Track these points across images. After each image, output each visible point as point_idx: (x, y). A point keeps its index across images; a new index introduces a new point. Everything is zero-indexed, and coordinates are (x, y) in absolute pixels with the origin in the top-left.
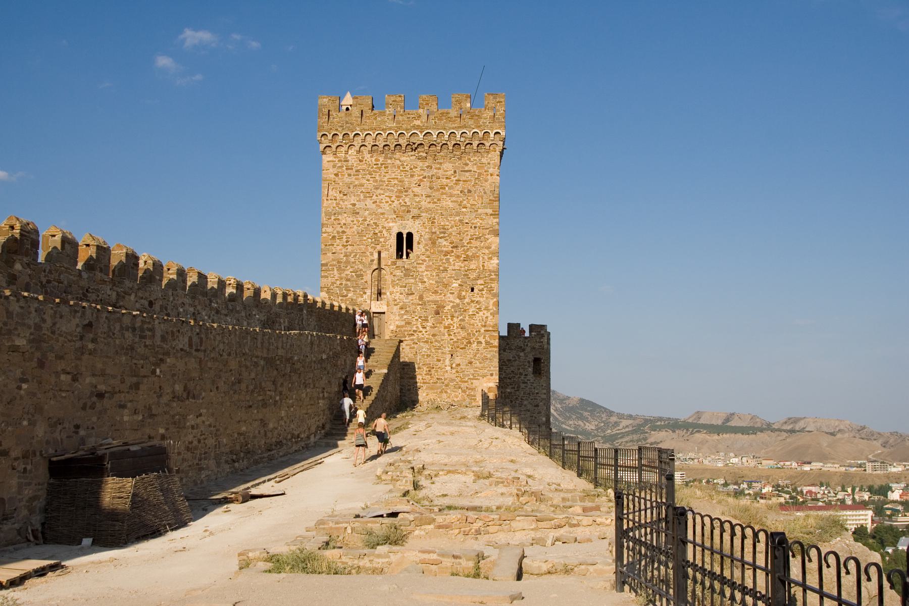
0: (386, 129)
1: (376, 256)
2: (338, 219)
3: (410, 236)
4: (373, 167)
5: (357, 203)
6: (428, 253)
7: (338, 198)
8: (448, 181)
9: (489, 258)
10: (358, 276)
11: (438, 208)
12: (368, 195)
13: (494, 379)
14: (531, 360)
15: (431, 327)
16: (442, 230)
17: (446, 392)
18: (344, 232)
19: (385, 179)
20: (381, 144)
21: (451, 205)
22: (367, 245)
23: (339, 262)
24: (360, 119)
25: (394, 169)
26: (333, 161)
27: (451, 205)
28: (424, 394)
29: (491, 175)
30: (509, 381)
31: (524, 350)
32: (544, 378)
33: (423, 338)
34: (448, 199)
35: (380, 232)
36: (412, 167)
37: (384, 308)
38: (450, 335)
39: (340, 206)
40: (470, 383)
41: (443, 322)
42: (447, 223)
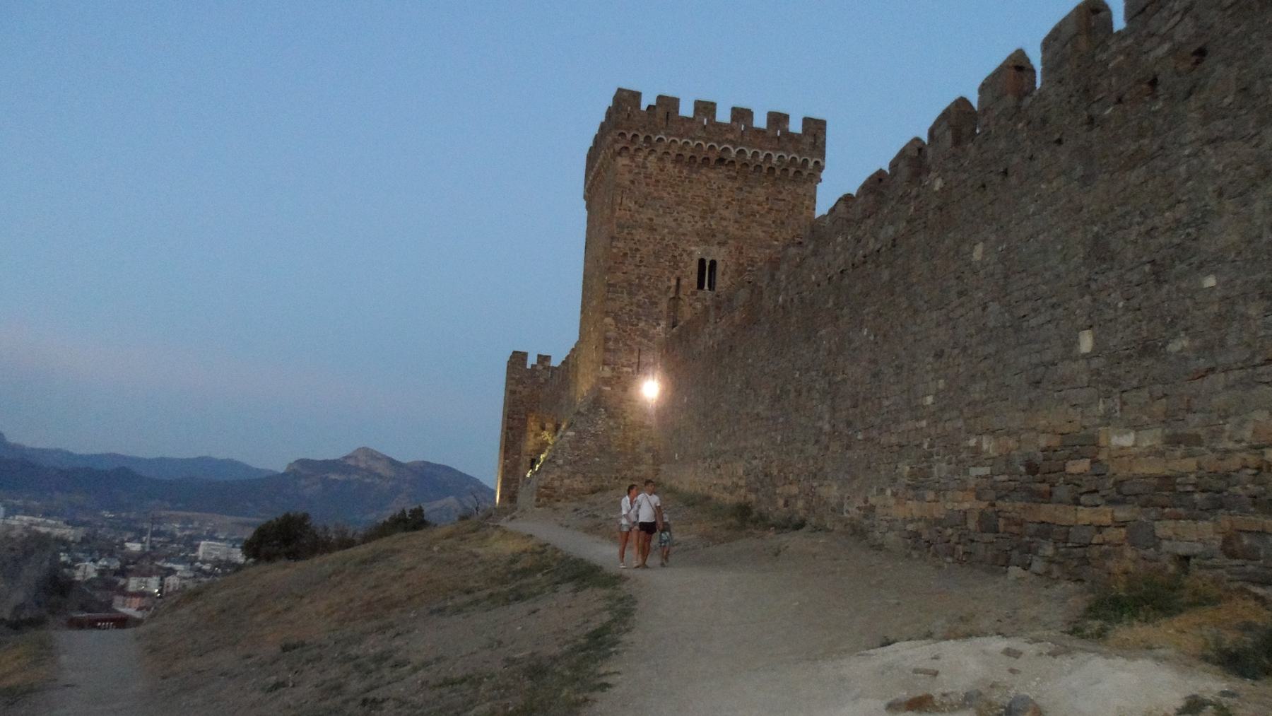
1: (674, 282)
2: (632, 234)
3: (713, 263)
4: (675, 180)
5: (654, 218)
7: (633, 209)
8: (760, 207)
16: (750, 263)
18: (637, 250)
20: (687, 154)
21: (761, 235)
22: (664, 269)
23: (630, 284)
24: (664, 123)
26: (627, 165)
27: (761, 235)
29: (807, 208)
36: (720, 186)
39: (634, 219)
42: (756, 256)
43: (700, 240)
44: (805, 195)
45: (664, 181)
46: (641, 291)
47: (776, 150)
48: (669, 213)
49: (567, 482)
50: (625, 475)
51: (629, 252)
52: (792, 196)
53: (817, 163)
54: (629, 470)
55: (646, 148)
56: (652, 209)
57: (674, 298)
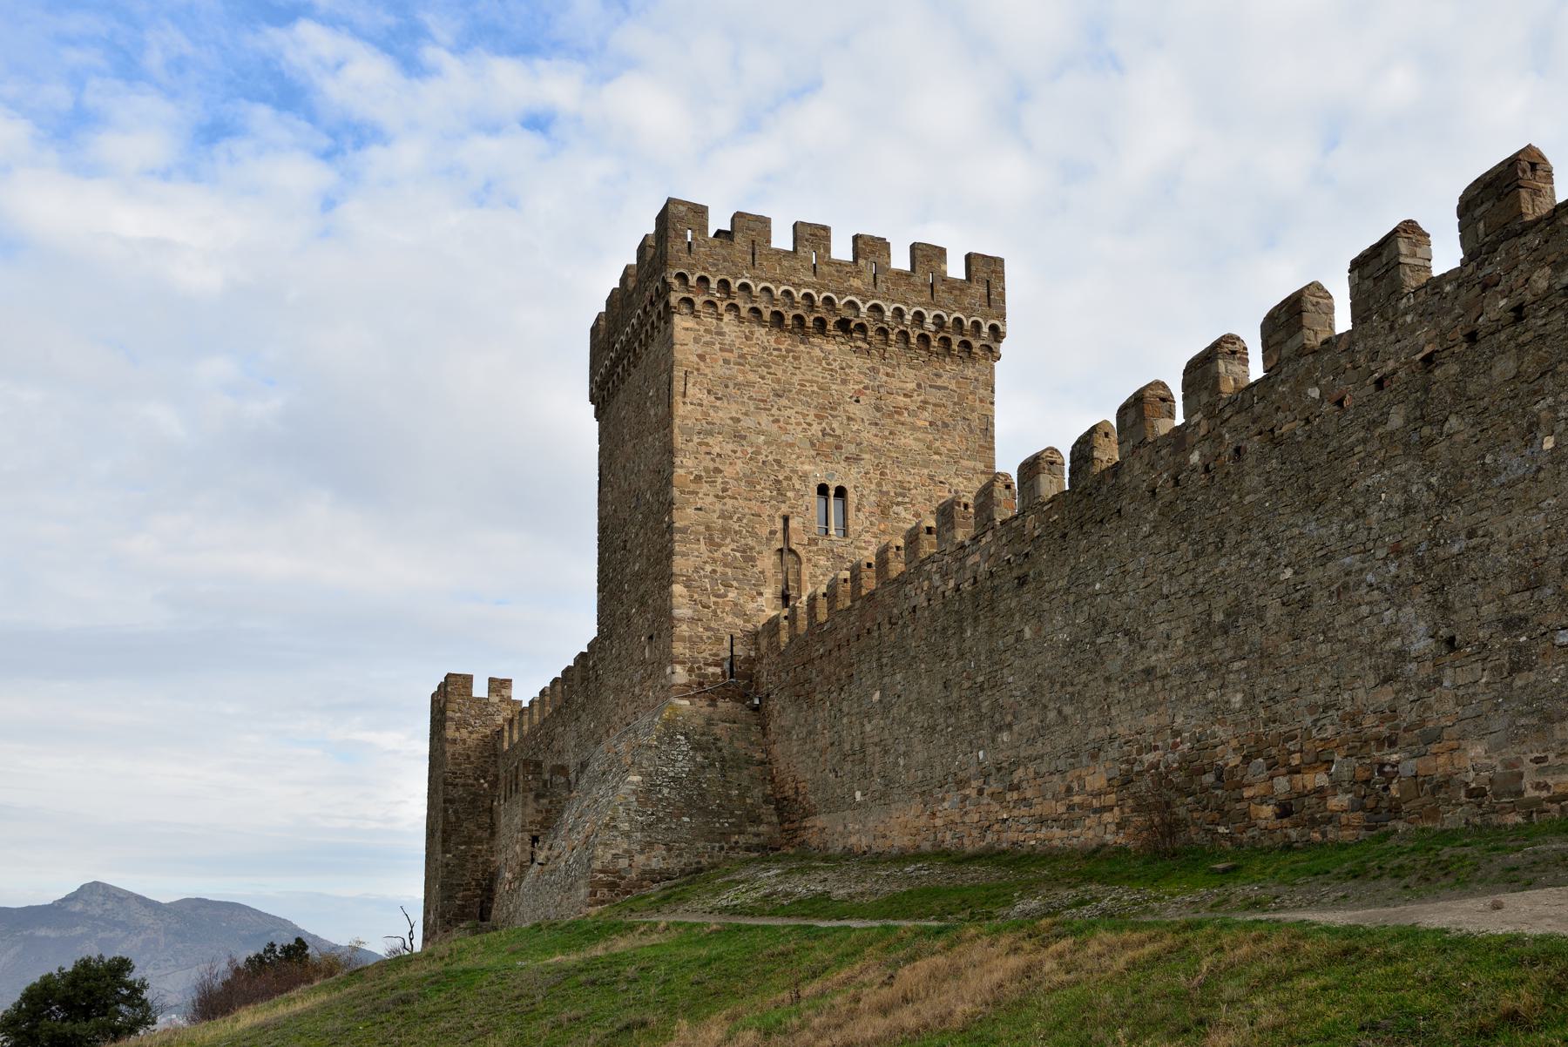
0: (800, 285)
1: (779, 525)
2: (707, 445)
3: (841, 492)
6: (875, 529)
7: (705, 403)
8: (908, 400)
12: (762, 405)
16: (899, 490)
21: (915, 445)
22: (762, 502)
23: (708, 528)
27: (915, 445)
34: (908, 433)
36: (844, 364)
39: (710, 419)
42: (908, 479)
43: (818, 454)
44: (976, 380)
45: (753, 356)
46: (729, 540)
47: (927, 305)
48: (765, 409)
49: (640, 859)
50: (736, 843)
51: (703, 474)
52: (958, 382)
53: (994, 328)
54: (740, 833)
55: (720, 299)
56: (736, 402)
57: (781, 550)
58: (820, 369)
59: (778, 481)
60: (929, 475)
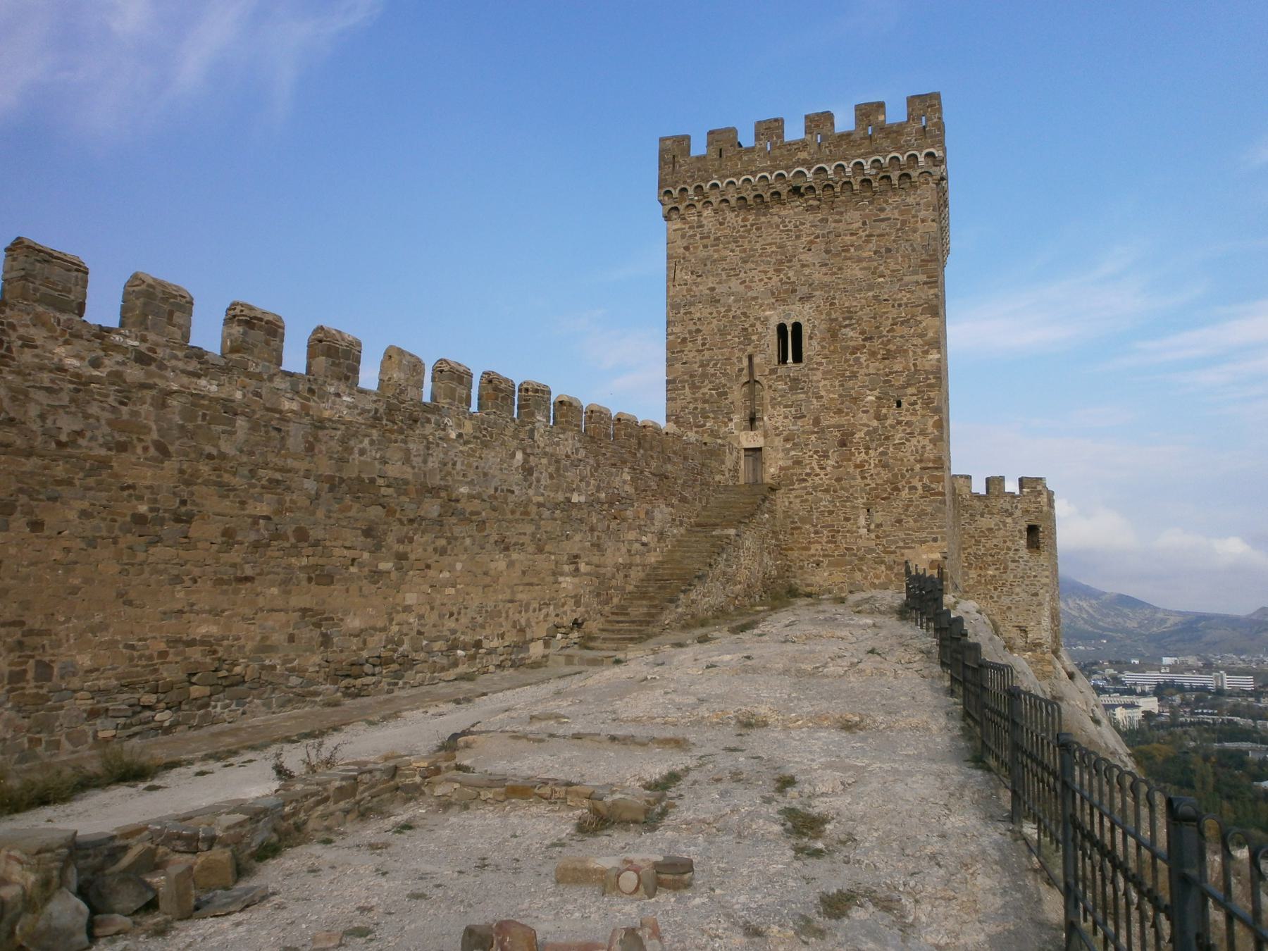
1: (745, 362)
2: (690, 313)
3: (797, 327)
4: (739, 231)
7: (689, 282)
8: (854, 238)
9: (923, 352)
10: (720, 395)
11: (839, 281)
12: (732, 273)
13: (939, 547)
14: (1022, 528)
15: (834, 467)
16: (847, 315)
17: (861, 570)
18: (698, 331)
19: (758, 246)
21: (859, 274)
23: (692, 376)
25: (770, 230)
27: (859, 274)
28: (826, 574)
29: (923, 221)
30: (990, 558)
31: (1011, 514)
32: (1044, 555)
33: (822, 485)
34: (854, 265)
35: (751, 326)
37: (759, 442)
38: (864, 478)
40: (898, 554)
41: (853, 458)
42: (855, 304)
44: (918, 204)
46: (707, 382)
53: (930, 155)
55: (698, 201)
57: (748, 382)
58: (778, 232)
59: (745, 329)
60: (874, 296)
